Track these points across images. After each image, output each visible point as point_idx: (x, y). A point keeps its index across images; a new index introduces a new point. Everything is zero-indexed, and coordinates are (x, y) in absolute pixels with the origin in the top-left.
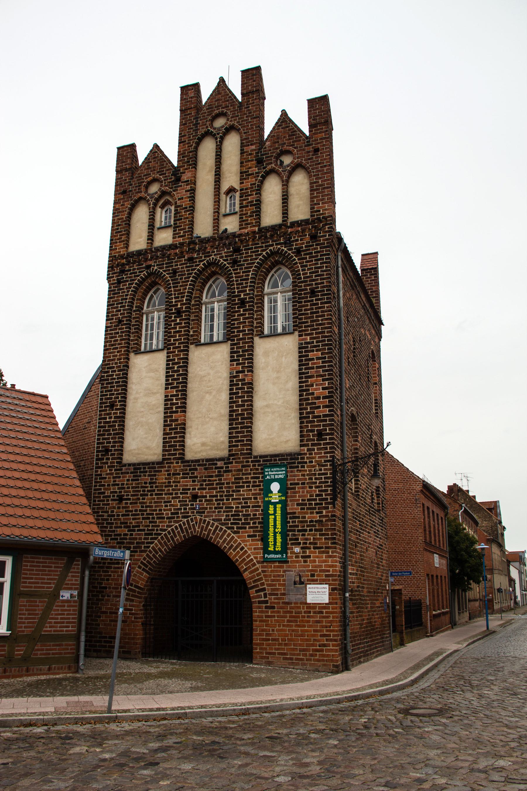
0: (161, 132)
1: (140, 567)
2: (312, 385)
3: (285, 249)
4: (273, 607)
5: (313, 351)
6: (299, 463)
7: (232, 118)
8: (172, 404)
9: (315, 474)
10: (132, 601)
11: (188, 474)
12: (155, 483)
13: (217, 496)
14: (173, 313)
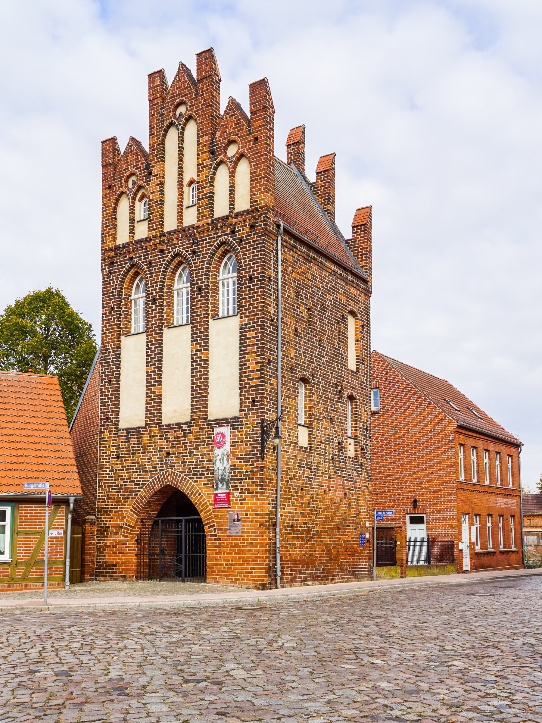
0: (133, 124)
1: (131, 510)
2: (249, 361)
3: (231, 239)
4: (220, 540)
5: (249, 331)
6: (239, 425)
7: (190, 107)
8: (151, 379)
9: (249, 434)
10: (127, 537)
13: (182, 453)
14: (150, 301)
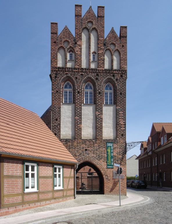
4: (110, 180)
5: (120, 111)
8: (78, 122)
11: (84, 143)
12: (73, 145)
13: (93, 150)
